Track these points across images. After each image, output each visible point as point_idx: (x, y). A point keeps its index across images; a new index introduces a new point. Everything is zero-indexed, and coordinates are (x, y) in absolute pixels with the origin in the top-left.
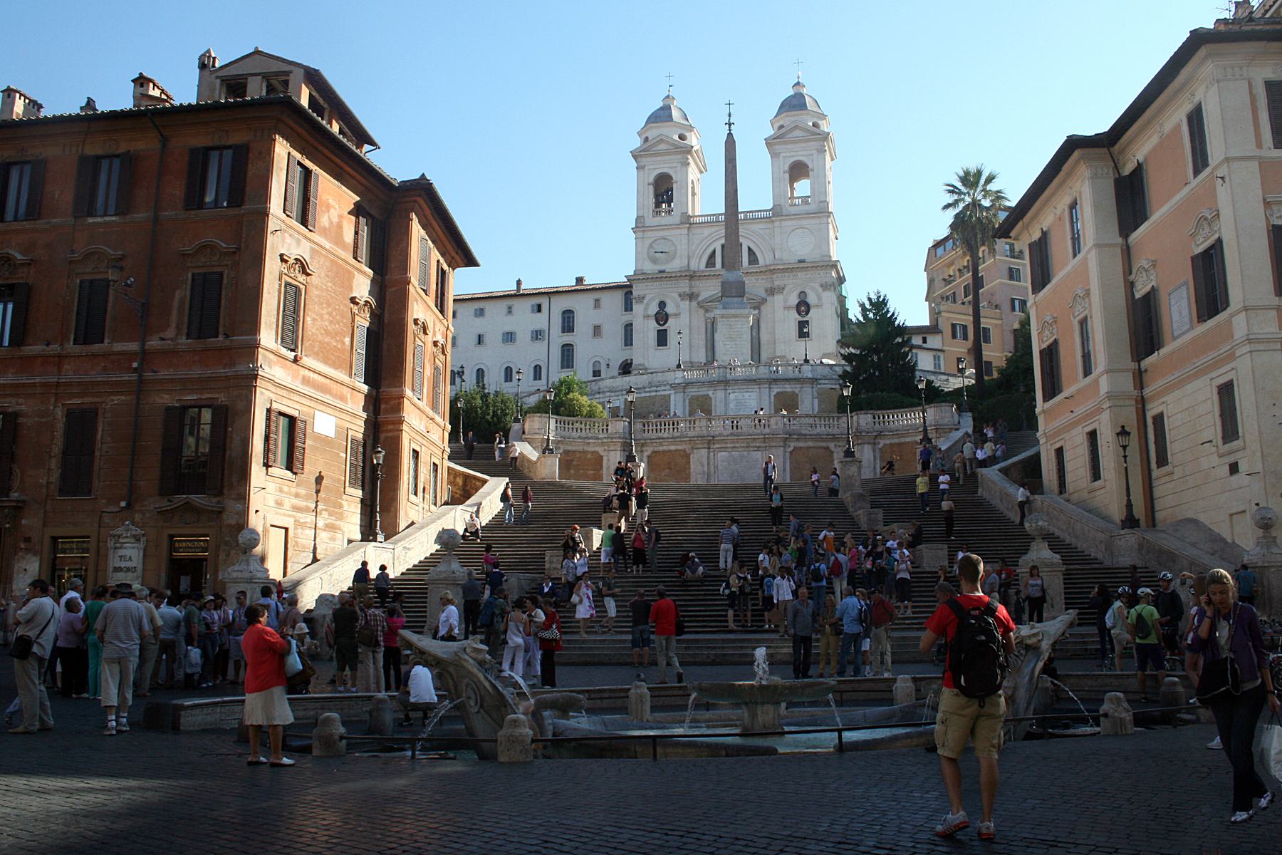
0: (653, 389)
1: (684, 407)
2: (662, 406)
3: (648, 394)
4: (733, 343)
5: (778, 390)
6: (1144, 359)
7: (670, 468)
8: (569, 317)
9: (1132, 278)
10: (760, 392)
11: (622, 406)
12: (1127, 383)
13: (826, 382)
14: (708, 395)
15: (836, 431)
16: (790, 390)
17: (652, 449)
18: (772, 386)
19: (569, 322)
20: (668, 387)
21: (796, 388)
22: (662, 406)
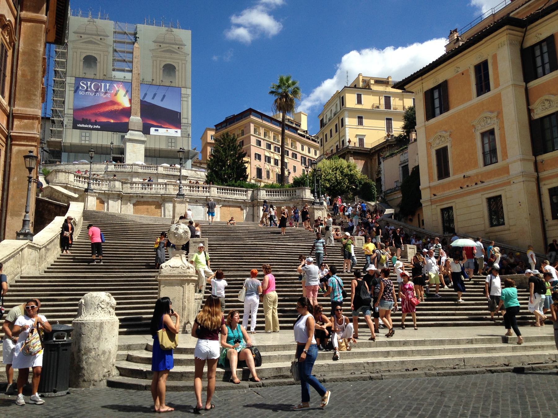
6: (541, 154)
7: (148, 212)
9: (530, 107)
12: (531, 167)
15: (245, 198)
17: (136, 199)
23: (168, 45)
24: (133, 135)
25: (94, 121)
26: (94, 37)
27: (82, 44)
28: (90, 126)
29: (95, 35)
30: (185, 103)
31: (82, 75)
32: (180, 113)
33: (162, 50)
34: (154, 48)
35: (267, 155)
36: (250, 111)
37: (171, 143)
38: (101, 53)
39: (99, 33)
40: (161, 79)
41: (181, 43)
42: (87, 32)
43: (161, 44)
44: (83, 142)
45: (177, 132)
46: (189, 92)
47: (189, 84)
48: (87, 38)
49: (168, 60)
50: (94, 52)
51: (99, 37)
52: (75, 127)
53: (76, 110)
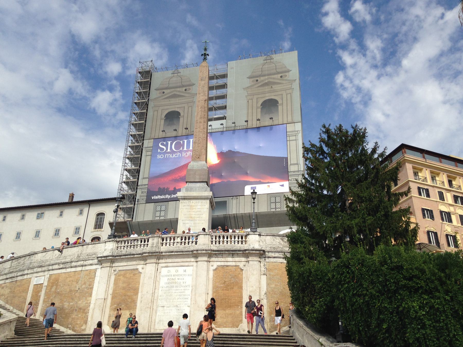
0: (79, 263)
1: (108, 287)
2: (85, 283)
3: (73, 270)
4: (192, 222)
5: (219, 264)
8: (101, 218)
10: (197, 266)
11: (46, 284)
13: (277, 255)
14: (137, 269)
16: (234, 264)
18: (213, 259)
19: (101, 221)
20: (96, 261)
21: (240, 261)
22: (85, 283)
23: (267, 77)
24: (191, 190)
25: (173, 189)
26: (178, 89)
27: (166, 100)
28: (168, 196)
29: (180, 87)
30: (293, 144)
31: (162, 135)
32: (287, 159)
33: (260, 84)
34: (250, 85)
35: (442, 210)
36: (403, 147)
37: (276, 202)
38: (186, 106)
39: (183, 84)
40: (259, 117)
41: (284, 70)
42: (171, 86)
43: (258, 79)
44: (157, 218)
45: (283, 186)
46: (298, 127)
47: (297, 117)
48: (170, 93)
49: (267, 95)
50: (177, 106)
51: (184, 88)
52: (149, 201)
53: (151, 179)
